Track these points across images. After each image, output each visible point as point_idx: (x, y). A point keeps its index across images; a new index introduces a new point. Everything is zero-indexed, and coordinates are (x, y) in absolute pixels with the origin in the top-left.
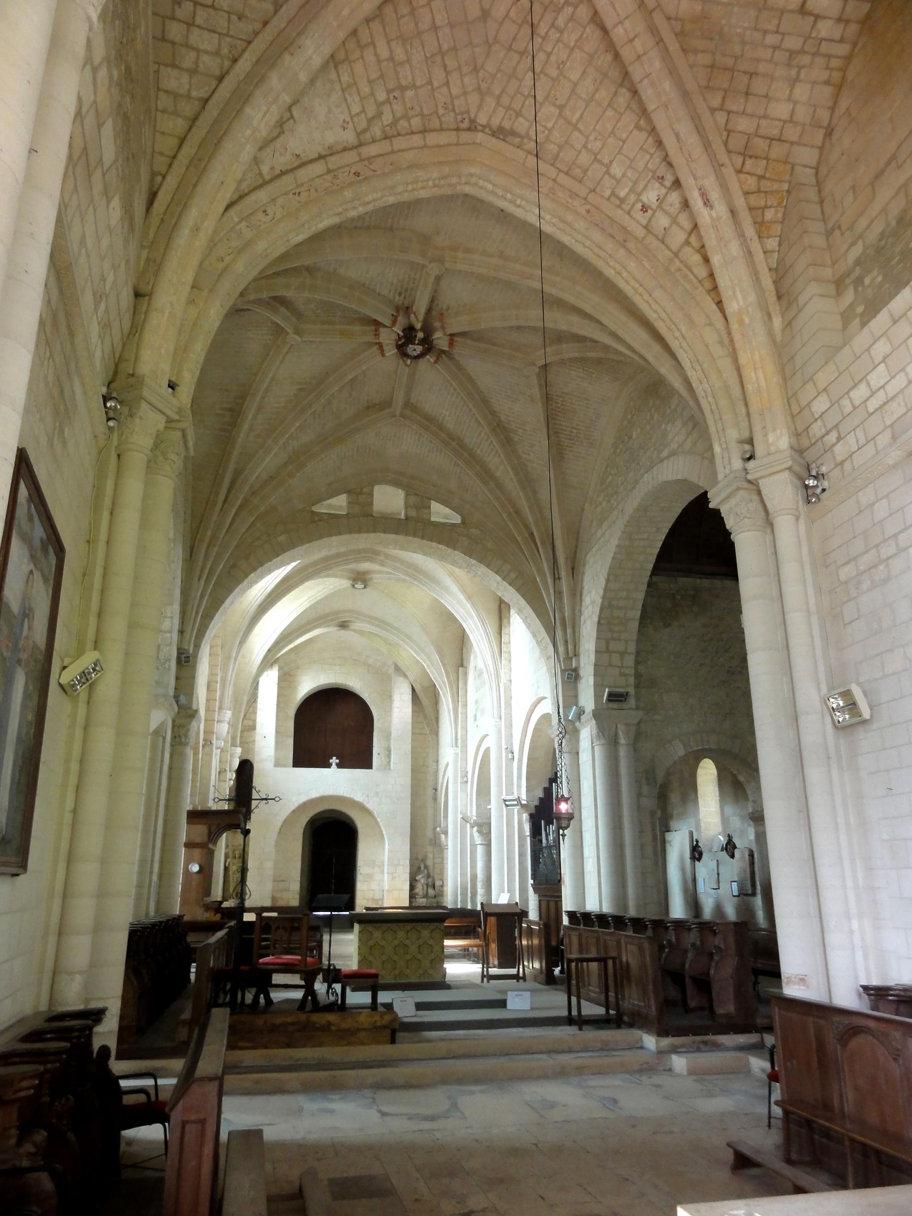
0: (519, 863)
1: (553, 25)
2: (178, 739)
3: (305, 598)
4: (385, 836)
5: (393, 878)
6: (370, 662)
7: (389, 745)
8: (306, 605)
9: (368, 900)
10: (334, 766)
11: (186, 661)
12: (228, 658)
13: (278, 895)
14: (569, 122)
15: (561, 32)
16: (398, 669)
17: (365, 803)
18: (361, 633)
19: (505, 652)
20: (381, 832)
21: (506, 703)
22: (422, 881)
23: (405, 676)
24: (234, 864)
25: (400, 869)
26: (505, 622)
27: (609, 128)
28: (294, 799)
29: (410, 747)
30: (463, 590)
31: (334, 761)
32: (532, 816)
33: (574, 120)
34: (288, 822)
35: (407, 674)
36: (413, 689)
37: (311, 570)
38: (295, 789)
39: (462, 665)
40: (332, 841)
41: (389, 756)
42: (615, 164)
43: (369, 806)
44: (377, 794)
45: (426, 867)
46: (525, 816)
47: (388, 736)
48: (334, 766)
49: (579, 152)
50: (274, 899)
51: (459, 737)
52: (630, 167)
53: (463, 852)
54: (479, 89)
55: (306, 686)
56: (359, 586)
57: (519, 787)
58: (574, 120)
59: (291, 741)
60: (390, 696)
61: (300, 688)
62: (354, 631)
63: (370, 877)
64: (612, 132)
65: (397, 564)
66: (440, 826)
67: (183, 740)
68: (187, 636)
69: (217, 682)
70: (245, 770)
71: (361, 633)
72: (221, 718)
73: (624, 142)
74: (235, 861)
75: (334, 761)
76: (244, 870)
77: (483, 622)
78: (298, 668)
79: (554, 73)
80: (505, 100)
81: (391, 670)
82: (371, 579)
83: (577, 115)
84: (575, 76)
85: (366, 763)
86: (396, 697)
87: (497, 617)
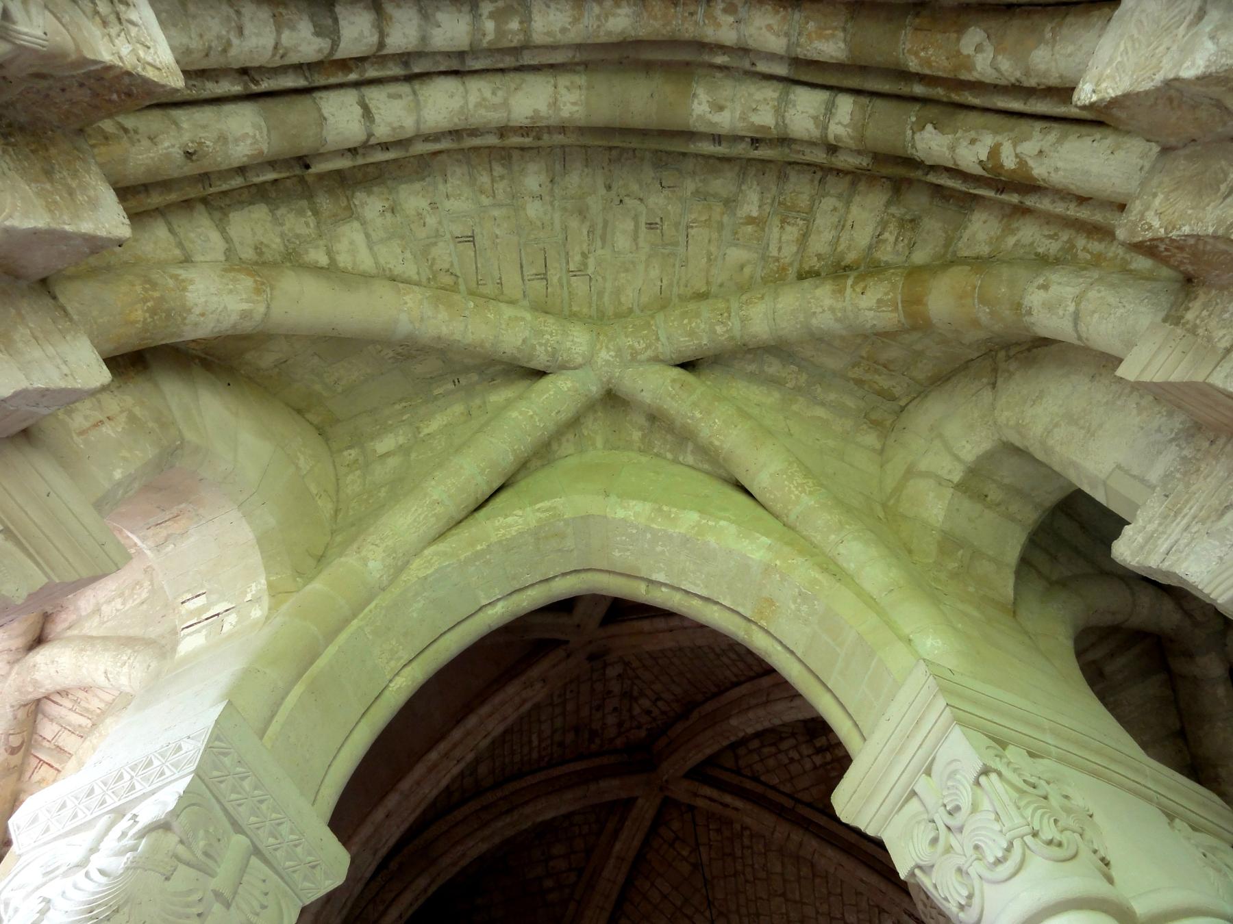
1: (743, 847)
14: (796, 902)
15: (750, 847)
27: (824, 891)
33: (798, 898)
42: (846, 915)
49: (817, 919)
52: (858, 912)
54: (721, 914)
58: (798, 898)
64: (829, 893)
73: (841, 895)
79: (763, 875)
80: (743, 911)
83: (797, 893)
84: (778, 869)
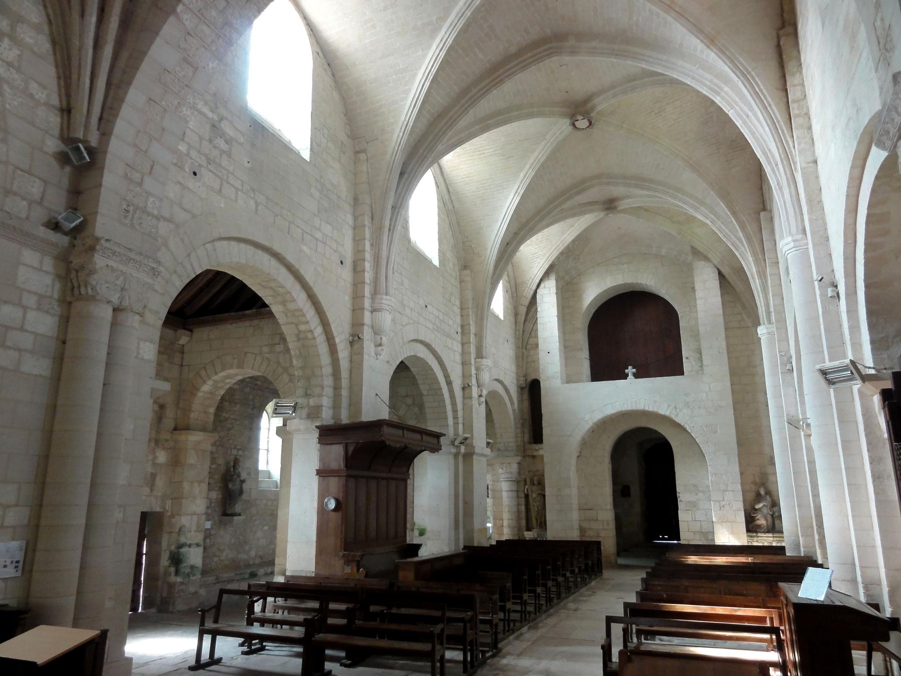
0: (876, 493)
2: (76, 292)
3: (528, 167)
5: (722, 507)
6: (663, 252)
7: (699, 345)
8: (531, 173)
10: (630, 376)
11: (81, 162)
12: (381, 228)
13: (586, 525)
16: (696, 252)
18: (636, 211)
19: (797, 116)
21: (809, 201)
22: (765, 510)
23: (706, 259)
24: (532, 492)
25: (729, 496)
26: (790, 67)
28: (587, 417)
30: (697, 29)
31: (630, 370)
32: (886, 395)
35: (709, 256)
36: (720, 274)
37: (474, 91)
39: (764, 209)
40: (646, 463)
43: (678, 420)
44: (687, 405)
45: (768, 493)
46: (876, 399)
47: (696, 336)
48: (630, 376)
50: (582, 530)
51: (772, 309)
53: (797, 473)
55: (593, 291)
56: (582, 123)
57: (857, 346)
59: (585, 354)
61: (585, 296)
62: (622, 211)
63: (694, 505)
65: (594, 44)
67: (83, 291)
68: (79, 116)
69: (364, 260)
70: (533, 390)
71: (636, 211)
72: (377, 306)
74: (534, 488)
76: (544, 496)
77: (744, 76)
78: (579, 275)
81: (690, 258)
82: (593, 108)
85: (678, 370)
86: (698, 286)
87: (773, 64)
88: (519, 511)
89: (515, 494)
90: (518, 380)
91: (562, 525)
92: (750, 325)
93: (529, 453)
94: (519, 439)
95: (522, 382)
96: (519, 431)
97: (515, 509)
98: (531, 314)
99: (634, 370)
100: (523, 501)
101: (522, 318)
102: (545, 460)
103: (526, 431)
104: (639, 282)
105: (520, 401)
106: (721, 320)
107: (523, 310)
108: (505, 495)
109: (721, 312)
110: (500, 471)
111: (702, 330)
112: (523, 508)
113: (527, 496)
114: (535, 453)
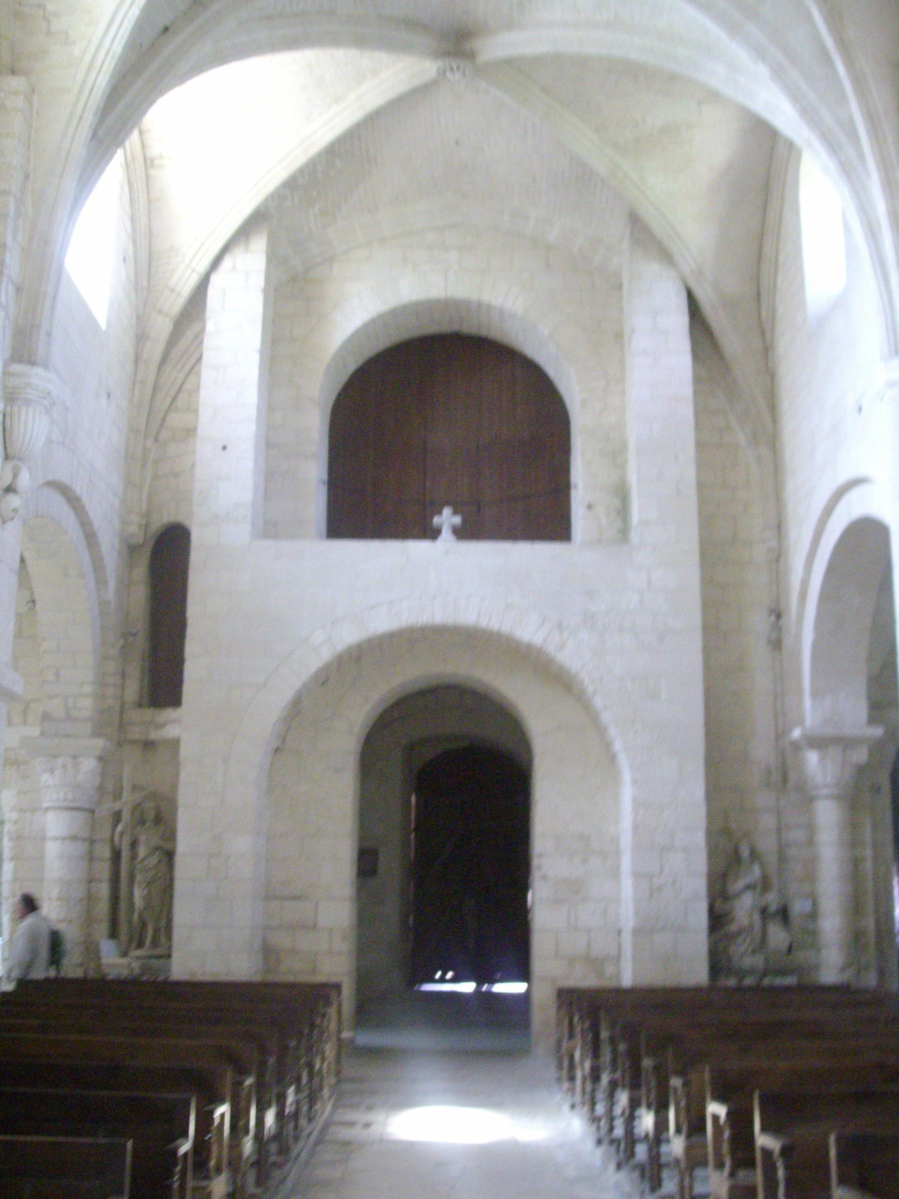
4: (624, 761)
9: (571, 961)
17: (551, 649)
20: (607, 746)
28: (319, 636)
29: (691, 473)
31: (447, 519)
34: (302, 714)
38: (324, 606)
41: (623, 512)
47: (616, 455)
60: (619, 336)
66: (800, 722)
70: (166, 556)
75: (447, 519)
88: (90, 898)
89: (81, 848)
90: (125, 523)
91: (210, 943)
92: (742, 440)
93: (135, 733)
94: (110, 691)
95: (133, 529)
96: (112, 667)
97: (79, 892)
98: (182, 344)
99: (457, 520)
100: (104, 870)
101: (155, 349)
102: (185, 751)
103: (135, 670)
104: (486, 298)
105: (125, 585)
106: (687, 412)
107: (162, 327)
108: (52, 849)
109: (687, 391)
110: (45, 778)
111: (634, 434)
112: (104, 889)
113: (116, 856)
114: (154, 735)
